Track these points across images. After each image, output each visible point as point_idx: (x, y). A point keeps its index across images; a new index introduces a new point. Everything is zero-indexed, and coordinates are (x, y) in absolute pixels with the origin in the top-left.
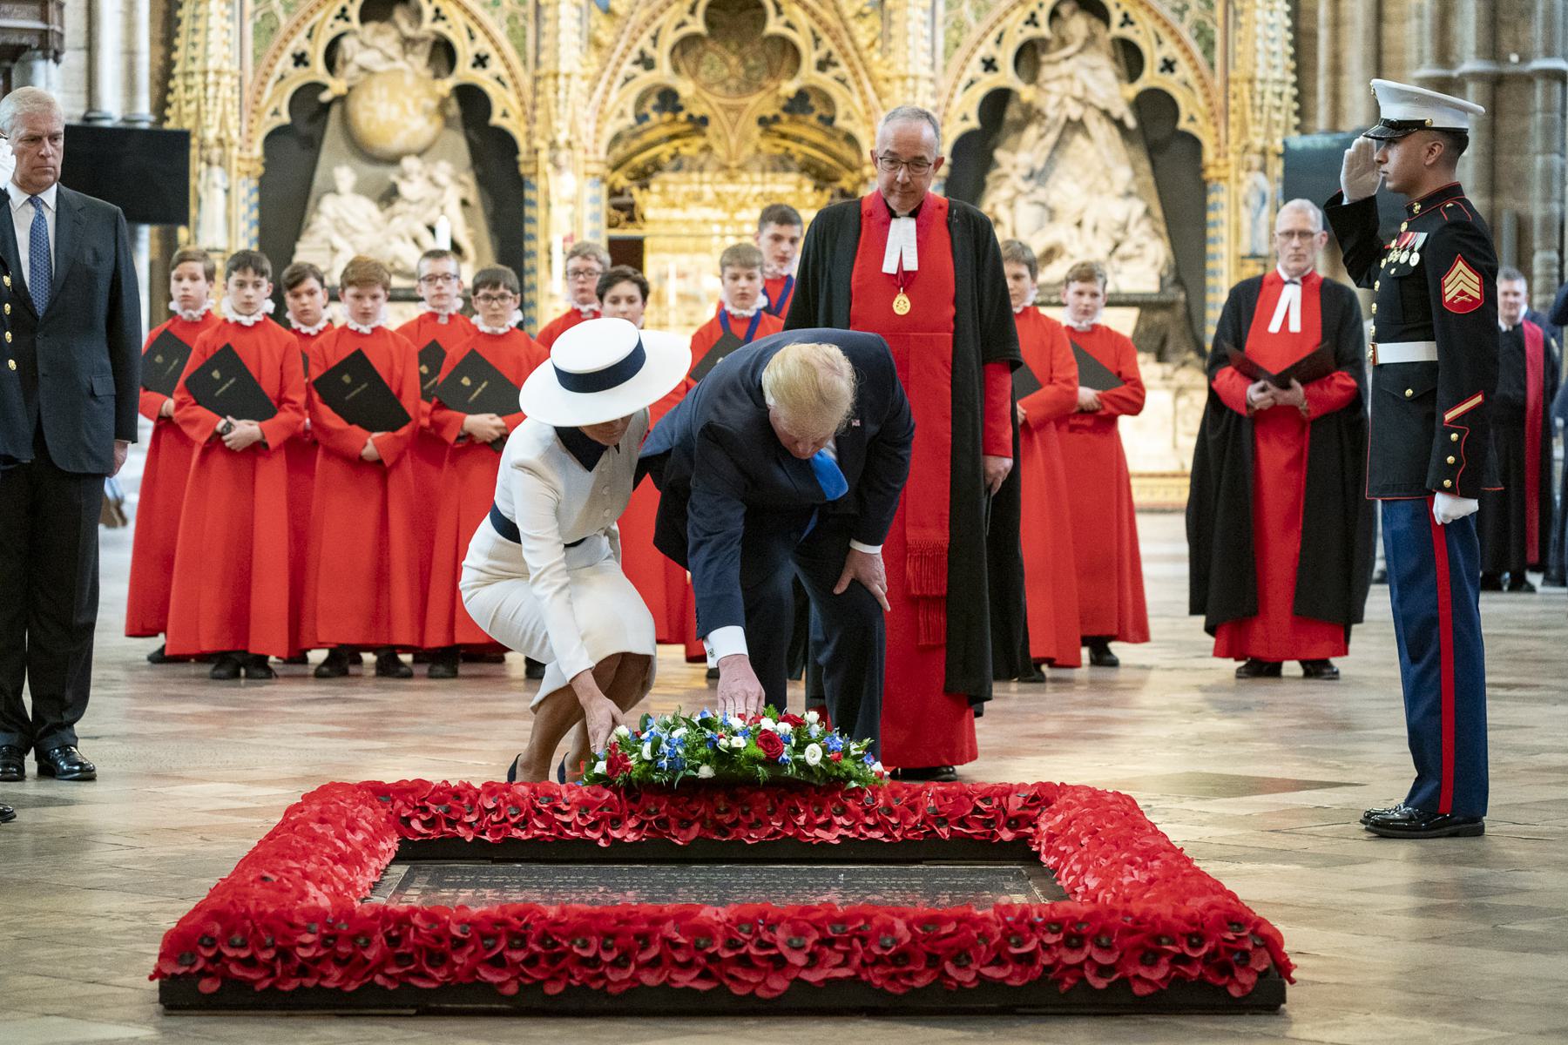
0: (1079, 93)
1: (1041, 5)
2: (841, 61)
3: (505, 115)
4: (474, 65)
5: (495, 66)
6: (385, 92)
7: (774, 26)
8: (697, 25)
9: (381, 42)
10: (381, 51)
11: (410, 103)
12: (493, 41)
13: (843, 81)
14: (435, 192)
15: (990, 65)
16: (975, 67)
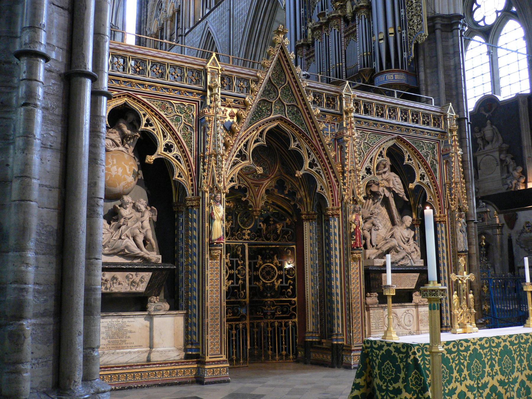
0: (391, 186)
1: (383, 149)
2: (318, 164)
3: (180, 176)
4: (165, 150)
5: (176, 151)
6: (115, 160)
7: (293, 146)
8: (263, 142)
9: (113, 136)
10: (112, 140)
11: (127, 168)
12: (176, 138)
13: (319, 173)
14: (138, 215)
15: (368, 171)
16: (363, 172)
